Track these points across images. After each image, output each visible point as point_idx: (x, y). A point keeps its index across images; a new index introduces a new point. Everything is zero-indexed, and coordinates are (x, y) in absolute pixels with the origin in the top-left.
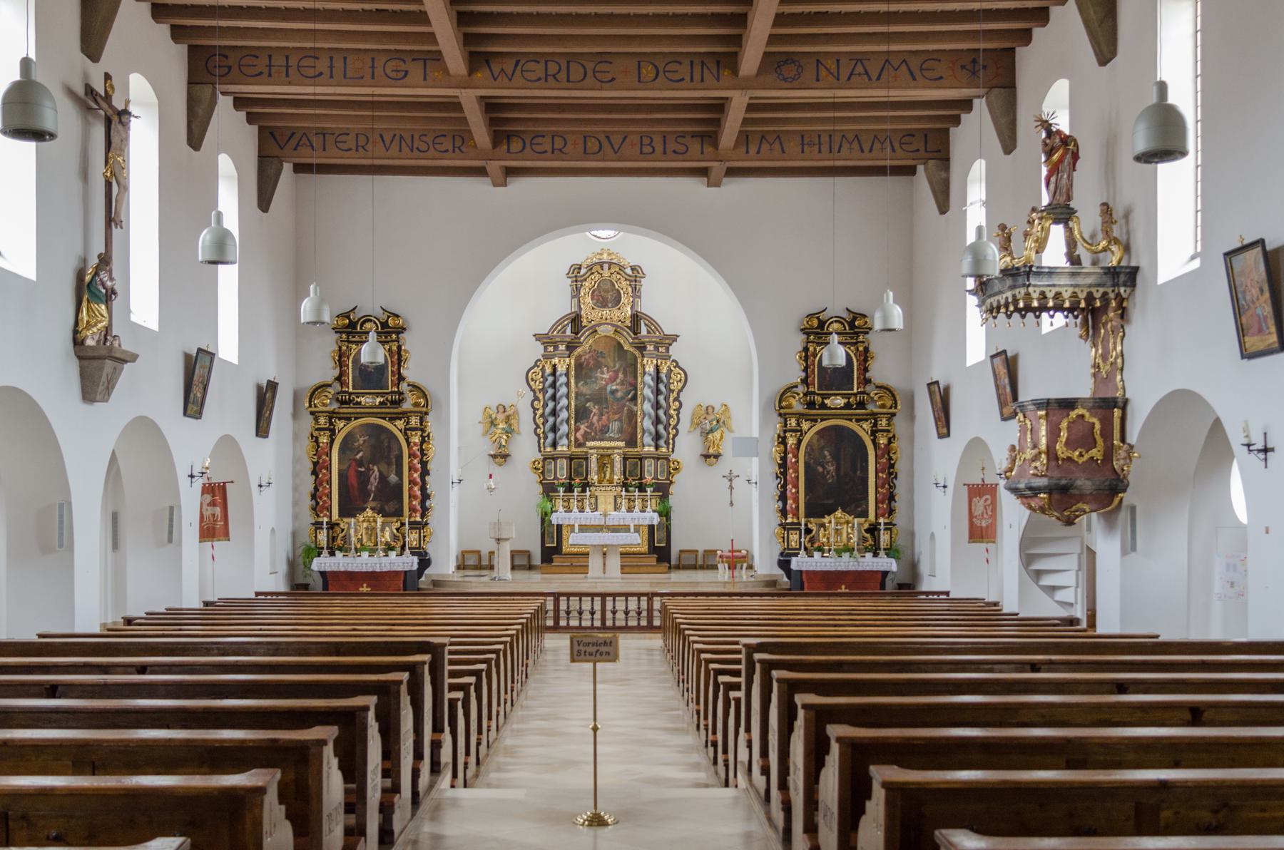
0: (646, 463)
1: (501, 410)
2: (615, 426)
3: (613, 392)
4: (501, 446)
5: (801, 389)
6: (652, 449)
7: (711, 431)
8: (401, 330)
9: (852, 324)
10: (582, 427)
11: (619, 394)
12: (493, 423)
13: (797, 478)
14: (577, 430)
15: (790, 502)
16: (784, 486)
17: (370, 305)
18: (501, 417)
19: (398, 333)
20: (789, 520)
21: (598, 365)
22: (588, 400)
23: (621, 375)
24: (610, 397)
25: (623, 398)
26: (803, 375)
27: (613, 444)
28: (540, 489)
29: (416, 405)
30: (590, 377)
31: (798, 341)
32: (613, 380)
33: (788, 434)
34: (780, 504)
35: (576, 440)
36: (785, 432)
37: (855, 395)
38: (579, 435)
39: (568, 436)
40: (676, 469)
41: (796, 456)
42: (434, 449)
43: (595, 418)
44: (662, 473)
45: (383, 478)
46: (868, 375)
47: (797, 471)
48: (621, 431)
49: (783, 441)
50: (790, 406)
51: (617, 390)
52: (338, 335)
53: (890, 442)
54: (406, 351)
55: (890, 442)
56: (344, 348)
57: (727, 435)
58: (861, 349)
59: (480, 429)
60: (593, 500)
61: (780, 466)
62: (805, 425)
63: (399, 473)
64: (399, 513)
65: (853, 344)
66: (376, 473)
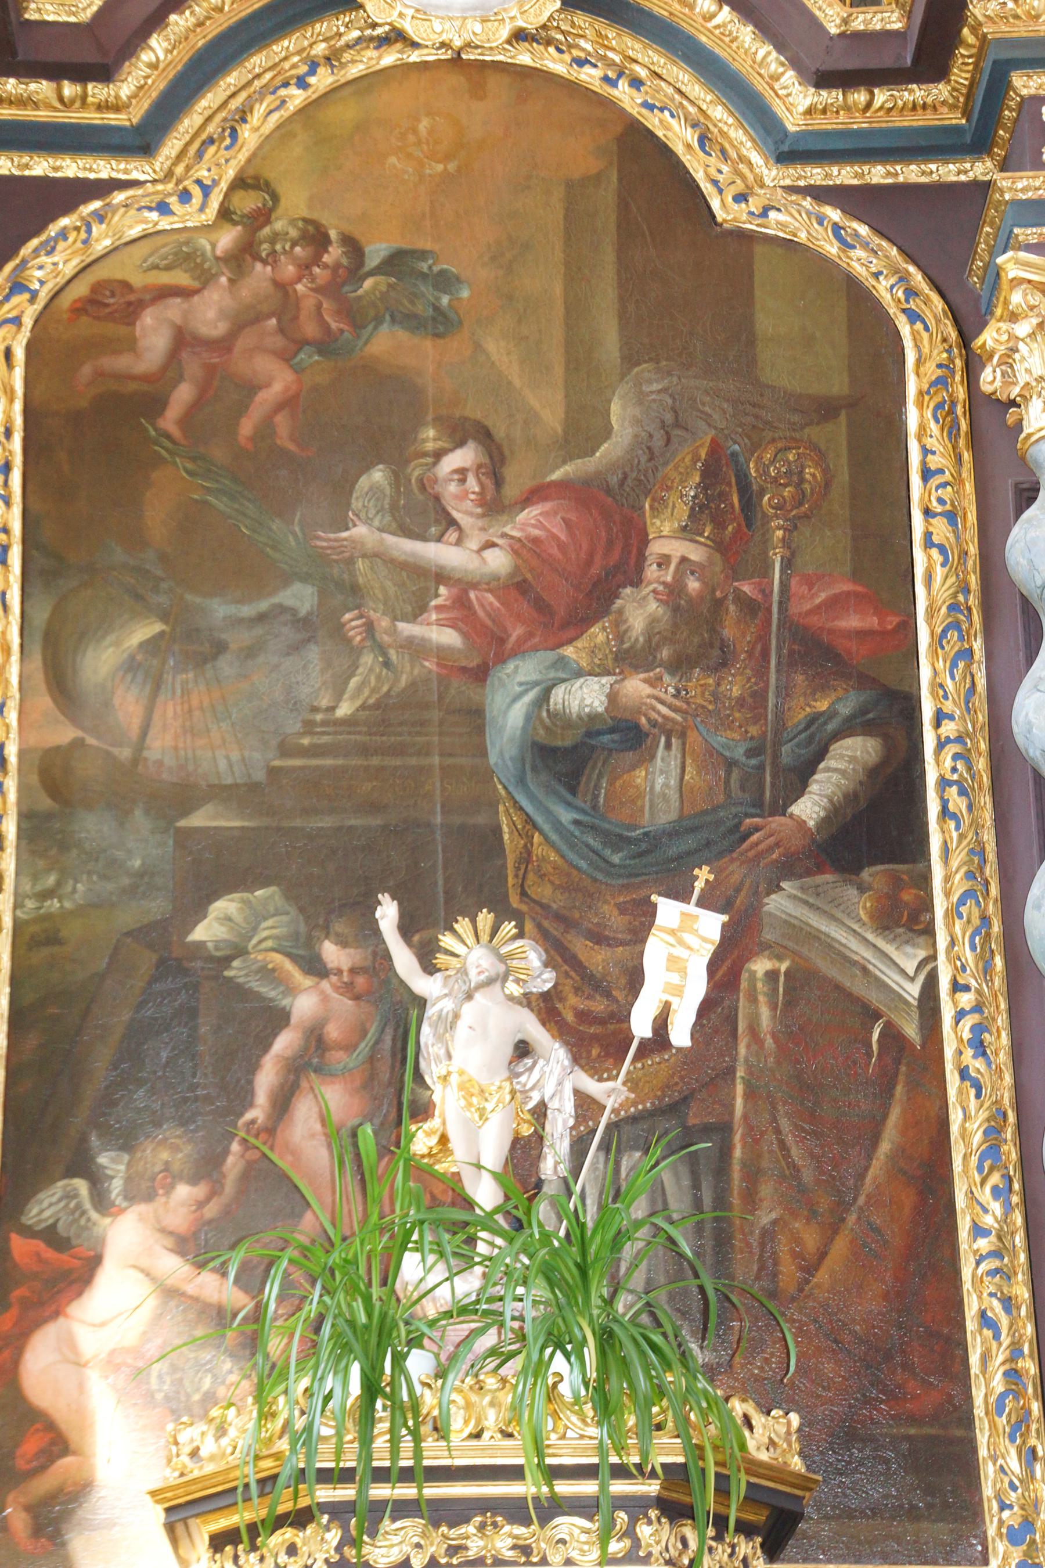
3: (569, 757)
11: (661, 784)
21: (365, 423)
23: (671, 543)
24: (536, 824)
30: (249, 569)
32: (562, 599)
51: (626, 734)
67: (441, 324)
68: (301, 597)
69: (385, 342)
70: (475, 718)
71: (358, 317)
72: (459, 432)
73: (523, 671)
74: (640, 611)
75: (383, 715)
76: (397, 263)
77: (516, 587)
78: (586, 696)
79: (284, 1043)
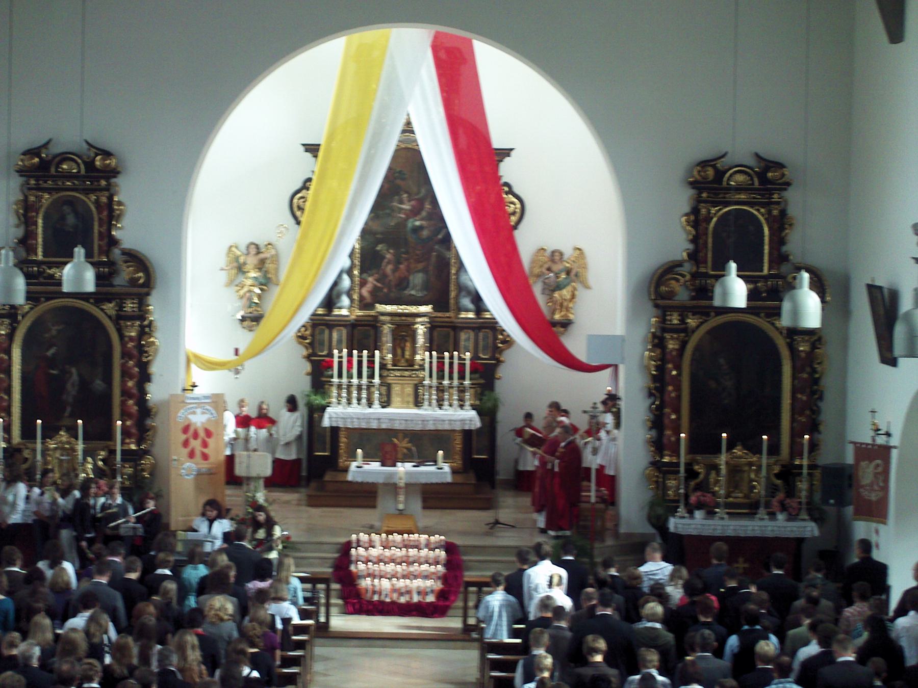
0: (463, 336)
1: (253, 250)
2: (418, 279)
3: (416, 230)
4: (251, 304)
5: (687, 268)
6: (471, 315)
7: (559, 287)
8: (113, 173)
9: (762, 176)
10: (370, 279)
11: (425, 233)
12: (240, 269)
13: (679, 397)
14: (363, 283)
15: (668, 432)
16: (660, 408)
17: (68, 132)
18: (252, 261)
19: (107, 179)
20: (666, 459)
22: (379, 242)
24: (411, 238)
25: (429, 238)
26: (691, 247)
27: (413, 309)
28: (308, 367)
29: (133, 282)
31: (683, 199)
32: (415, 212)
33: (667, 336)
34: (654, 433)
35: (362, 298)
36: (664, 330)
37: (766, 278)
38: (365, 292)
39: (349, 294)
40: (504, 342)
41: (678, 367)
42: (158, 339)
43: (389, 269)
44: (485, 348)
45: (84, 385)
46: (784, 249)
47: (678, 389)
48: (426, 286)
49: (658, 341)
50: (671, 295)
51: (421, 228)
52: (23, 179)
53: (814, 347)
54: (120, 203)
55: (814, 347)
56: (32, 198)
57: (581, 292)
58: (775, 212)
59: (223, 277)
60: (384, 389)
61: (655, 378)
62: (692, 322)
63: (108, 380)
64: (108, 434)
65: (763, 205)
66: (75, 377)
67: (403, 179)
68: (388, 211)
69: (398, 182)
70: (405, 226)
71: (395, 178)
72: (406, 192)
73: (411, 220)
74: (424, 214)
75: (398, 225)
76: (400, 172)
77: (411, 211)
78: (418, 223)
79: (386, 260)
